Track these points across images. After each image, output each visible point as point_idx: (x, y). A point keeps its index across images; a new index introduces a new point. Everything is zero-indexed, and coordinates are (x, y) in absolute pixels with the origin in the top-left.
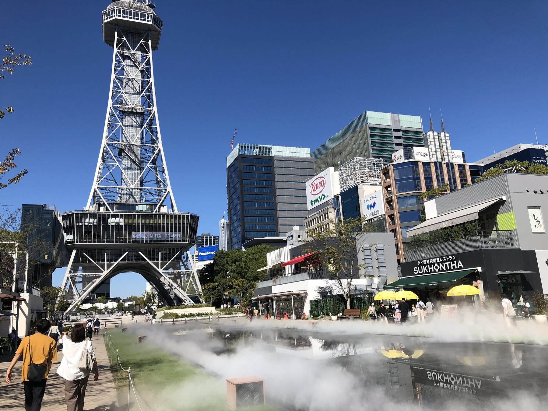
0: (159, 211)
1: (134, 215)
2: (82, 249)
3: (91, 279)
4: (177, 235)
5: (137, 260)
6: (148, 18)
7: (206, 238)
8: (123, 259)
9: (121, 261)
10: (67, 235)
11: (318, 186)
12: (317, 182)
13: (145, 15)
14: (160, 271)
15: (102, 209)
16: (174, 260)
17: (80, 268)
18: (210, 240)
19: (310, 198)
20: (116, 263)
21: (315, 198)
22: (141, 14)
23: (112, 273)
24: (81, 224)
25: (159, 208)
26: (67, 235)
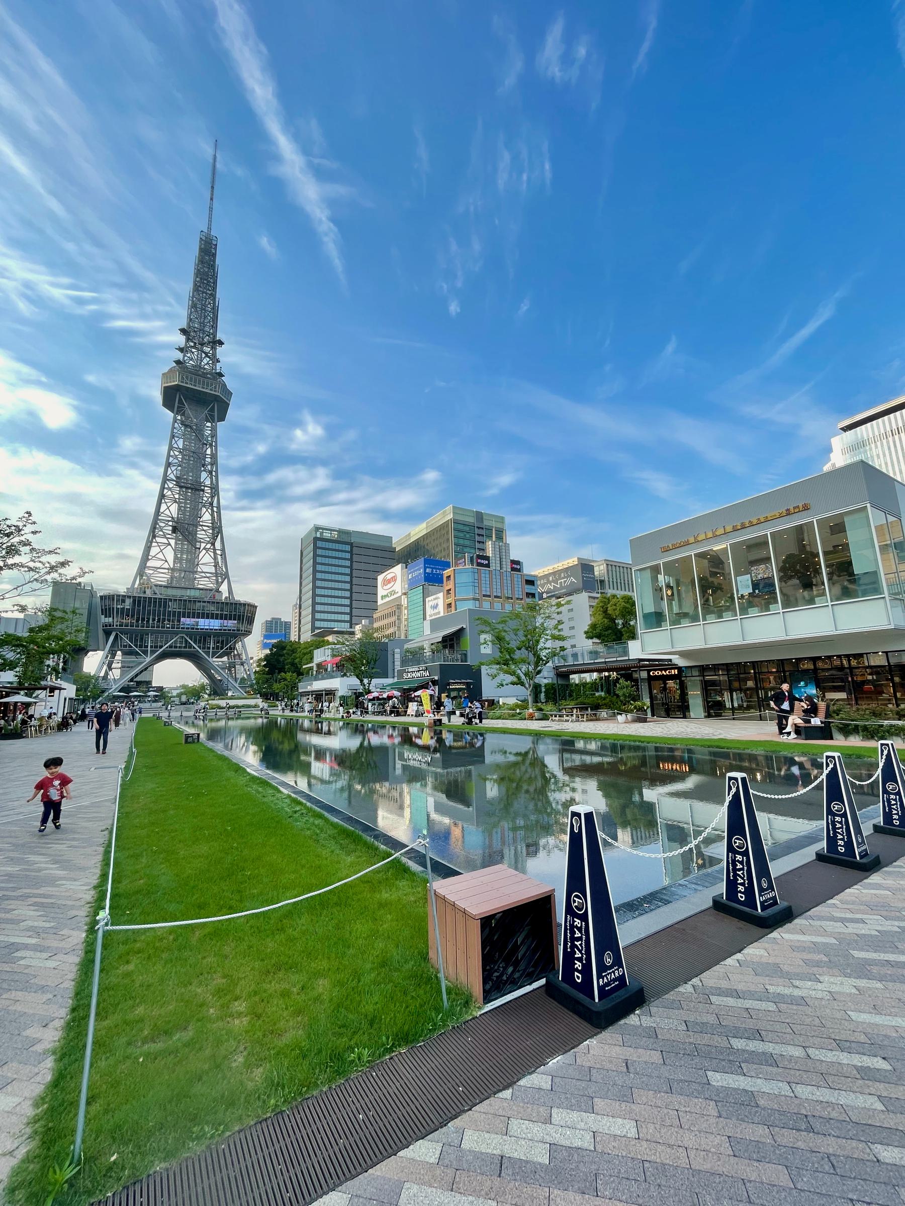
4: (231, 624)
8: (171, 646)
11: (389, 581)
12: (389, 577)
14: (210, 660)
17: (119, 653)
19: (381, 592)
21: (385, 593)
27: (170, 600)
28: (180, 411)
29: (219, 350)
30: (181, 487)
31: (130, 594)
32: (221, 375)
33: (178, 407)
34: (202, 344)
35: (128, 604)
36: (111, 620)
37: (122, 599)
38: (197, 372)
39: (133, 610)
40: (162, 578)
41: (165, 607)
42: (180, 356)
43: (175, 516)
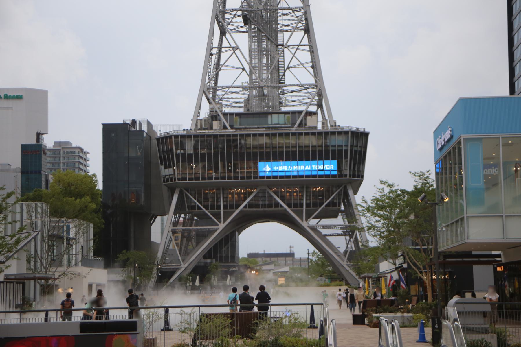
3: (202, 236)
5: (270, 206)
8: (250, 205)
9: (245, 207)
10: (166, 168)
15: (215, 124)
20: (237, 211)
24: (182, 151)
26: (166, 168)
31: (193, 133)
40: (234, 102)
41: (236, 147)
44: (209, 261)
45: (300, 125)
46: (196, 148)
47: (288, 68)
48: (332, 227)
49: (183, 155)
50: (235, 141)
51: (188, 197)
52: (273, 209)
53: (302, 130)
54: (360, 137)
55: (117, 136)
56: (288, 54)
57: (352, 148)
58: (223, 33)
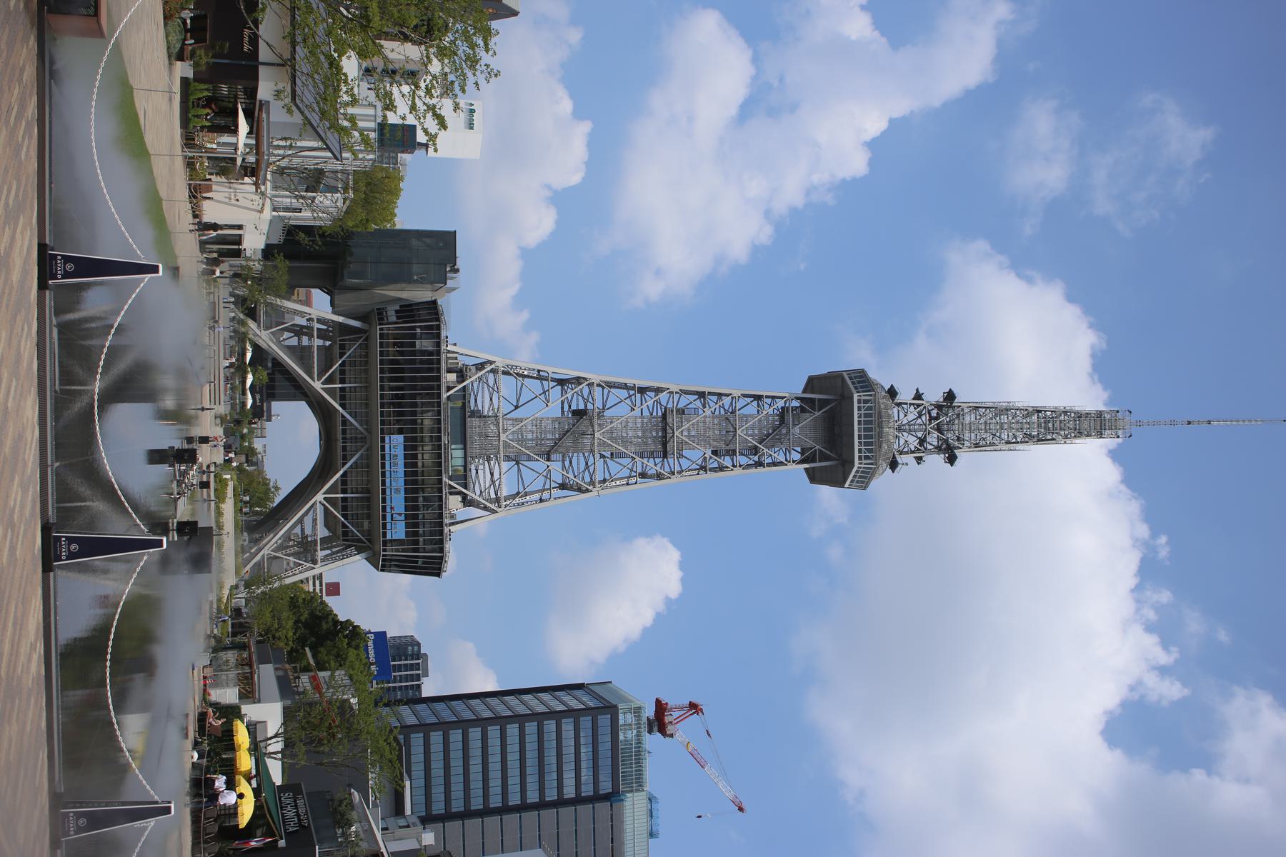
0: (451, 494)
1: (439, 439)
2: (367, 339)
4: (398, 531)
5: (344, 449)
6: (867, 458)
7: (417, 667)
8: (345, 422)
10: (397, 312)
13: (870, 451)
14: (320, 497)
15: (452, 377)
16: (344, 526)
18: (412, 678)
22: (871, 443)
23: (318, 403)
25: (460, 493)
26: (397, 312)
27: (439, 413)
28: (807, 404)
29: (939, 459)
30: (664, 416)
31: (443, 347)
32: (894, 465)
33: (812, 400)
34: (939, 429)
35: (424, 344)
36: (394, 319)
37: (435, 333)
38: (875, 422)
39: (414, 353)
42: (905, 395)
43: (607, 413)
44: (270, 365)
45: (451, 487)
46: (423, 353)
47: (518, 463)
48: (312, 518)
49: (414, 336)
50: (432, 404)
51: (356, 340)
52: (340, 453)
53: (445, 490)
54: (434, 567)
55: (438, 252)
56: (541, 465)
57: (422, 555)
58: (561, 382)
